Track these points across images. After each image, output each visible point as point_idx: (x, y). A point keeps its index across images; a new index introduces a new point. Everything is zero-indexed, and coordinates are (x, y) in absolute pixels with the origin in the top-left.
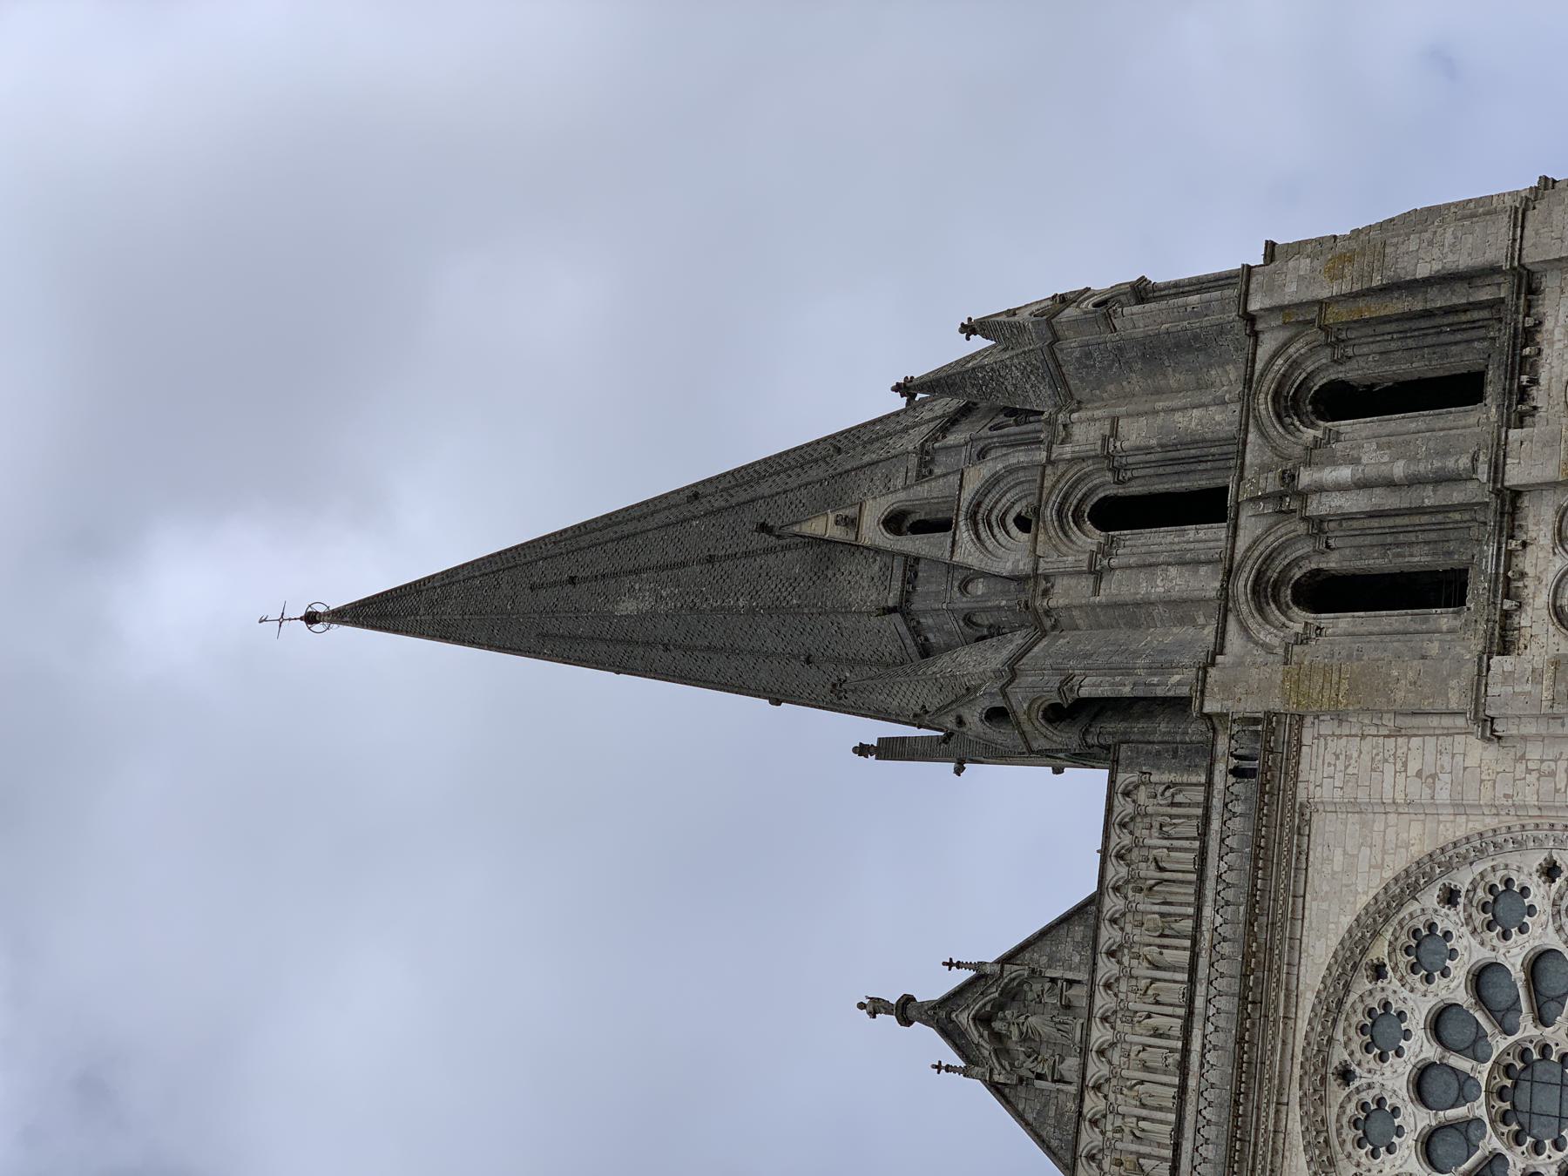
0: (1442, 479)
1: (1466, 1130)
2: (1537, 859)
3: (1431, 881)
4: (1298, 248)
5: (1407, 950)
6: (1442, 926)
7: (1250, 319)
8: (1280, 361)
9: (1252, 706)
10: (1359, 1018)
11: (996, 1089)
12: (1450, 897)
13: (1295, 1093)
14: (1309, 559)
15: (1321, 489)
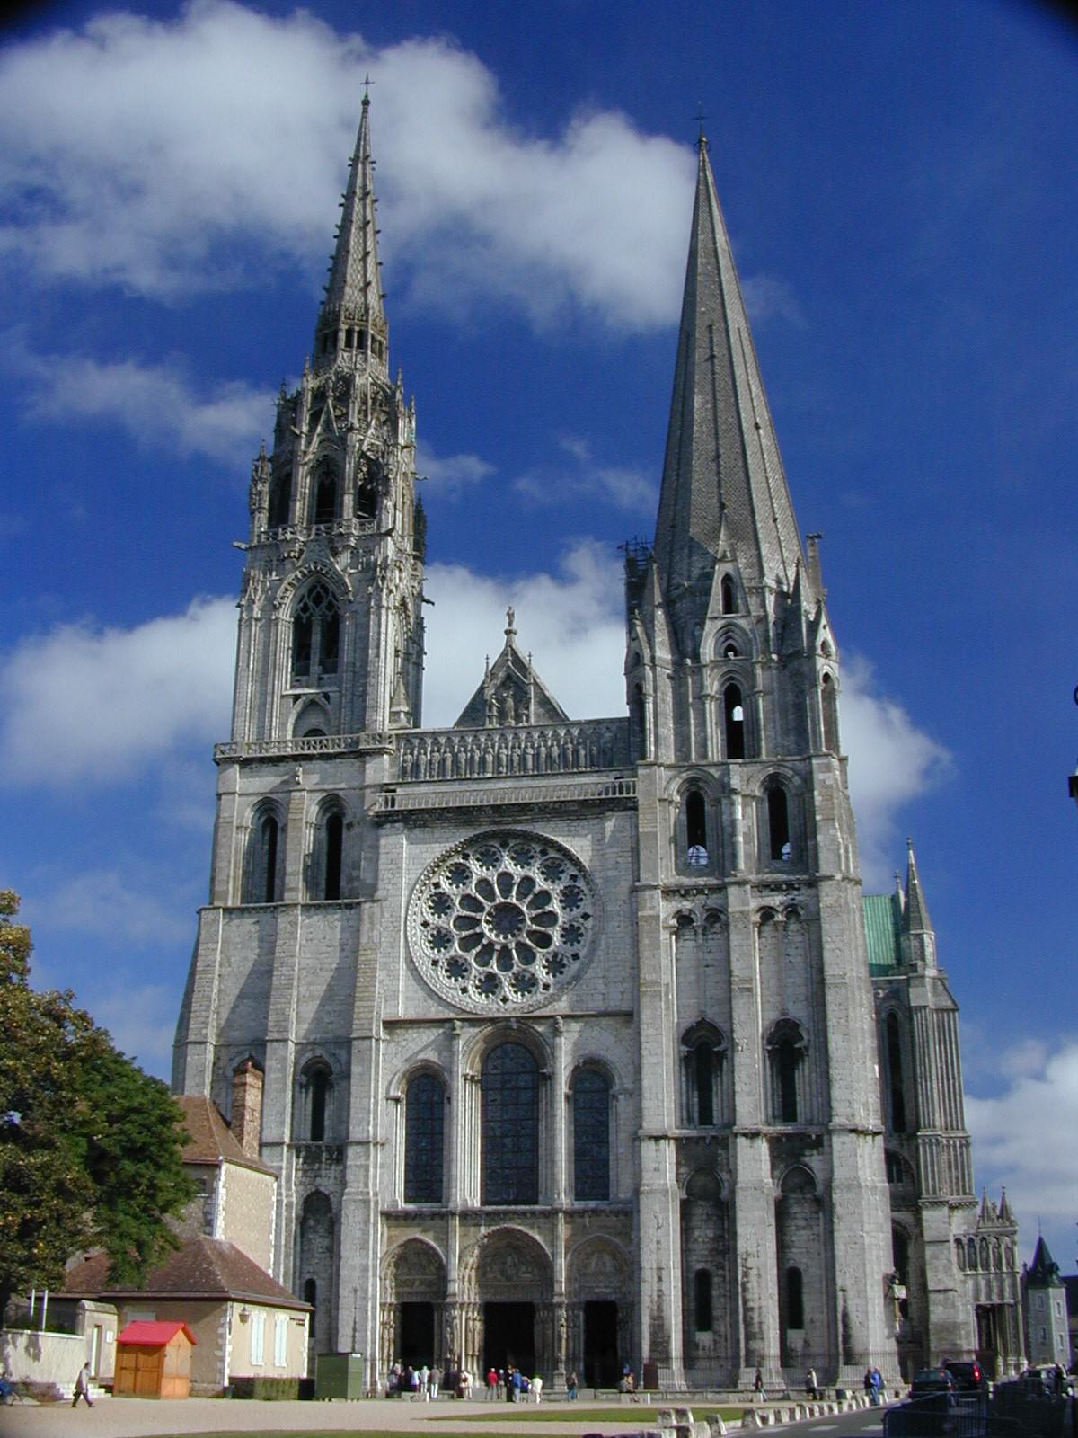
0: (734, 856)
1: (490, 896)
2: (590, 912)
3: (580, 871)
4: (844, 772)
5: (553, 863)
6: (562, 876)
7: (810, 758)
8: (791, 773)
9: (640, 786)
10: (526, 848)
11: (482, 688)
12: (573, 878)
13: (495, 828)
14: (709, 796)
15: (733, 804)
